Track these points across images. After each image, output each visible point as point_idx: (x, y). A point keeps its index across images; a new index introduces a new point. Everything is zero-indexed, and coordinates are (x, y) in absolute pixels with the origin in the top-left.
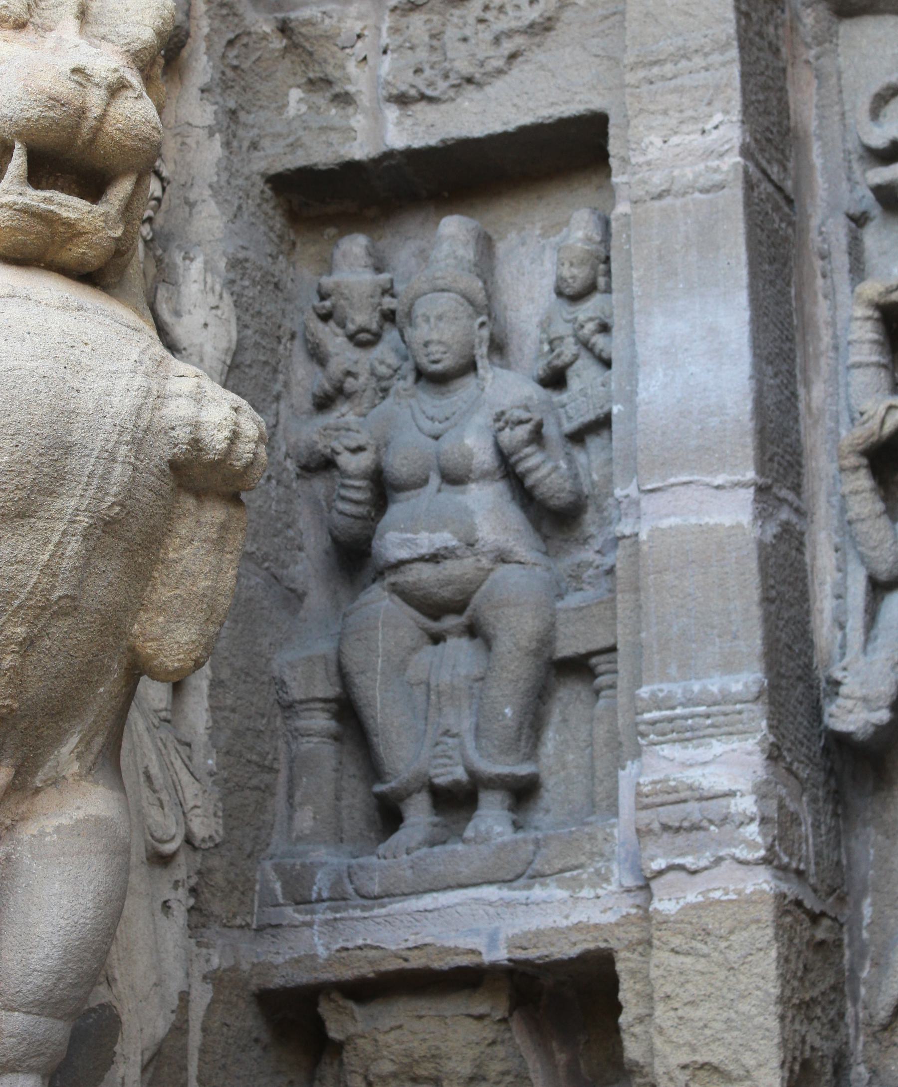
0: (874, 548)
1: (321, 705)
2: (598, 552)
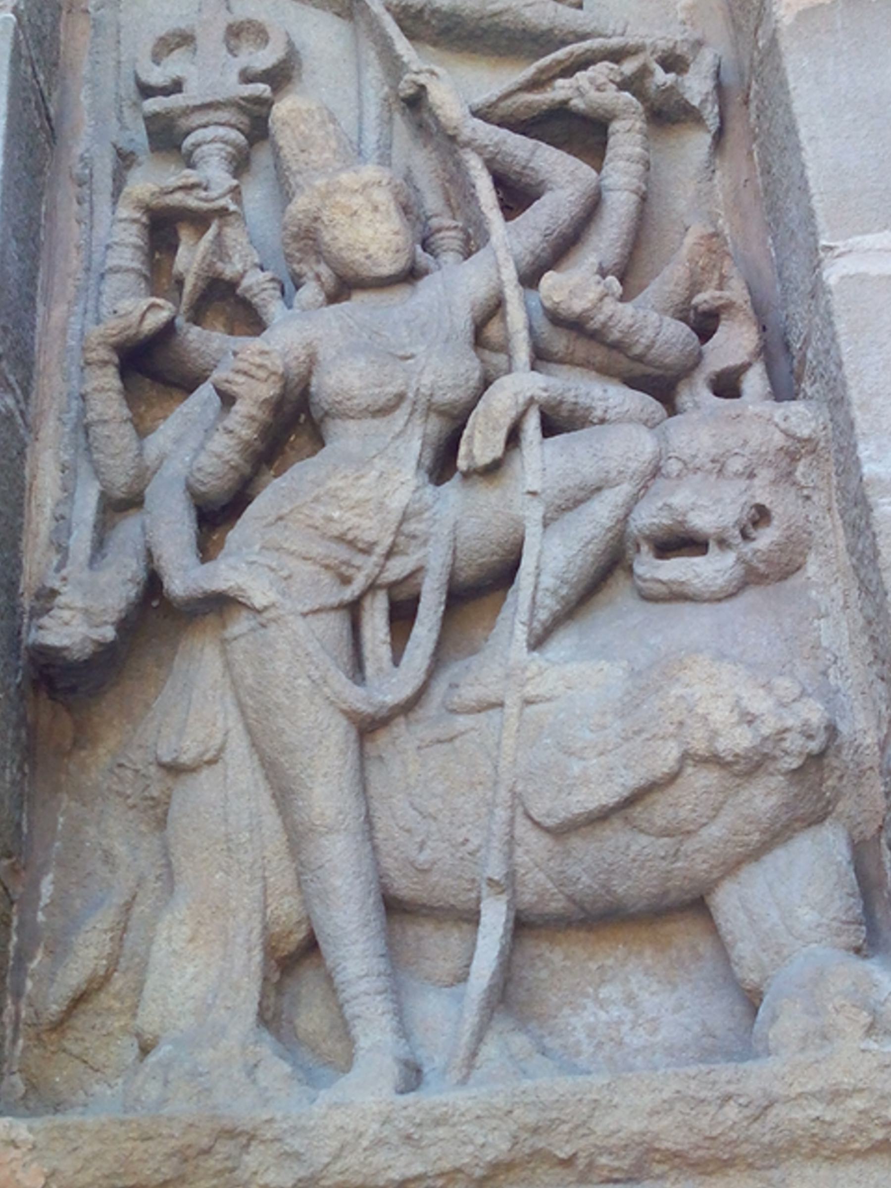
0: (113, 456)
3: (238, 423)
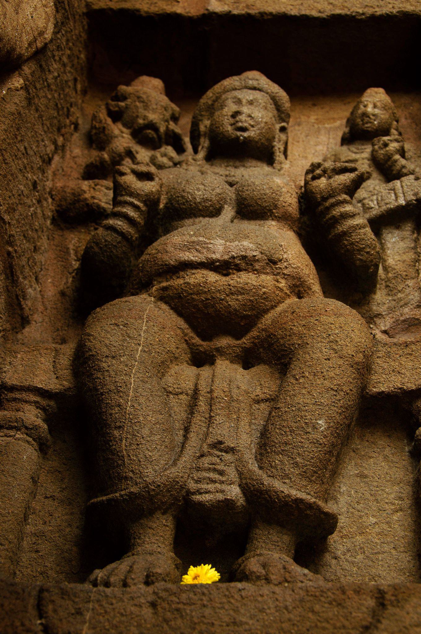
1: (38, 399)
2: (385, 332)
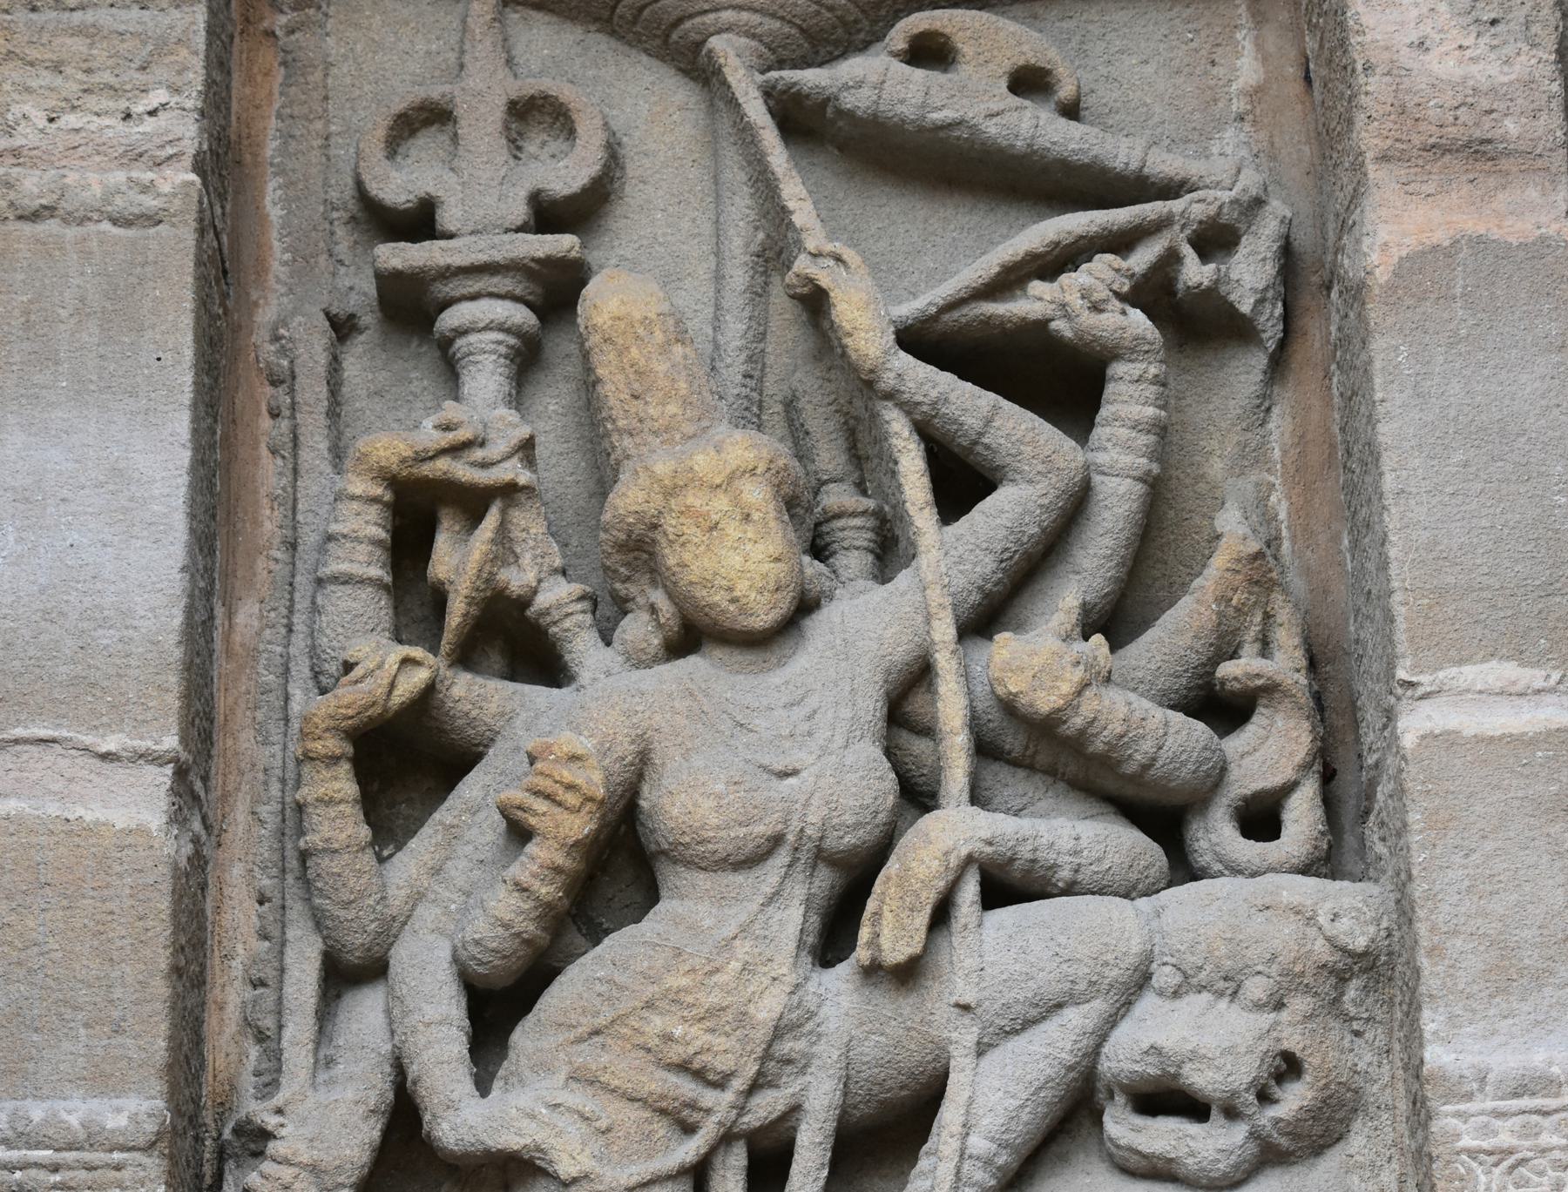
0: (347, 905)
3: (535, 876)
